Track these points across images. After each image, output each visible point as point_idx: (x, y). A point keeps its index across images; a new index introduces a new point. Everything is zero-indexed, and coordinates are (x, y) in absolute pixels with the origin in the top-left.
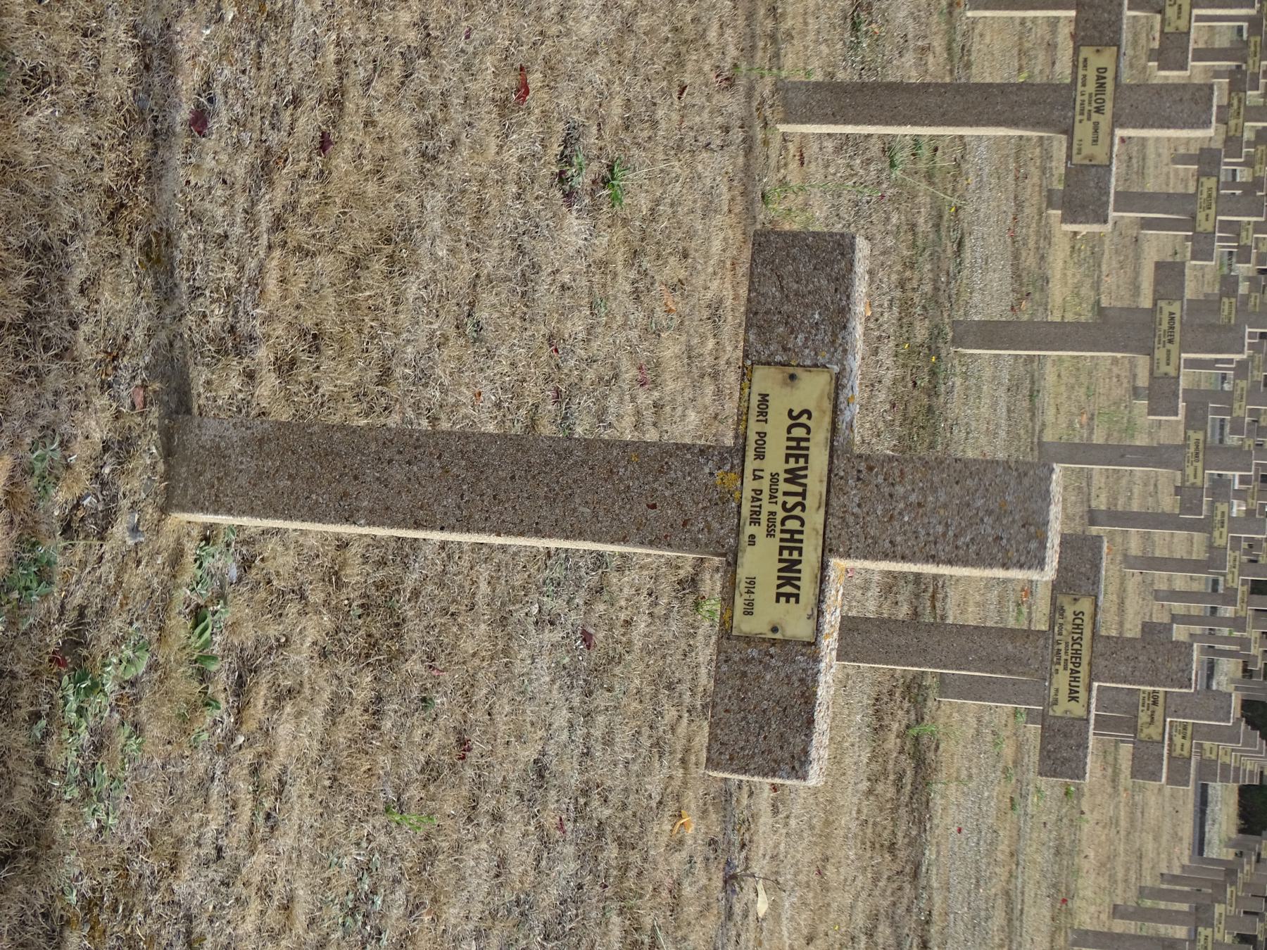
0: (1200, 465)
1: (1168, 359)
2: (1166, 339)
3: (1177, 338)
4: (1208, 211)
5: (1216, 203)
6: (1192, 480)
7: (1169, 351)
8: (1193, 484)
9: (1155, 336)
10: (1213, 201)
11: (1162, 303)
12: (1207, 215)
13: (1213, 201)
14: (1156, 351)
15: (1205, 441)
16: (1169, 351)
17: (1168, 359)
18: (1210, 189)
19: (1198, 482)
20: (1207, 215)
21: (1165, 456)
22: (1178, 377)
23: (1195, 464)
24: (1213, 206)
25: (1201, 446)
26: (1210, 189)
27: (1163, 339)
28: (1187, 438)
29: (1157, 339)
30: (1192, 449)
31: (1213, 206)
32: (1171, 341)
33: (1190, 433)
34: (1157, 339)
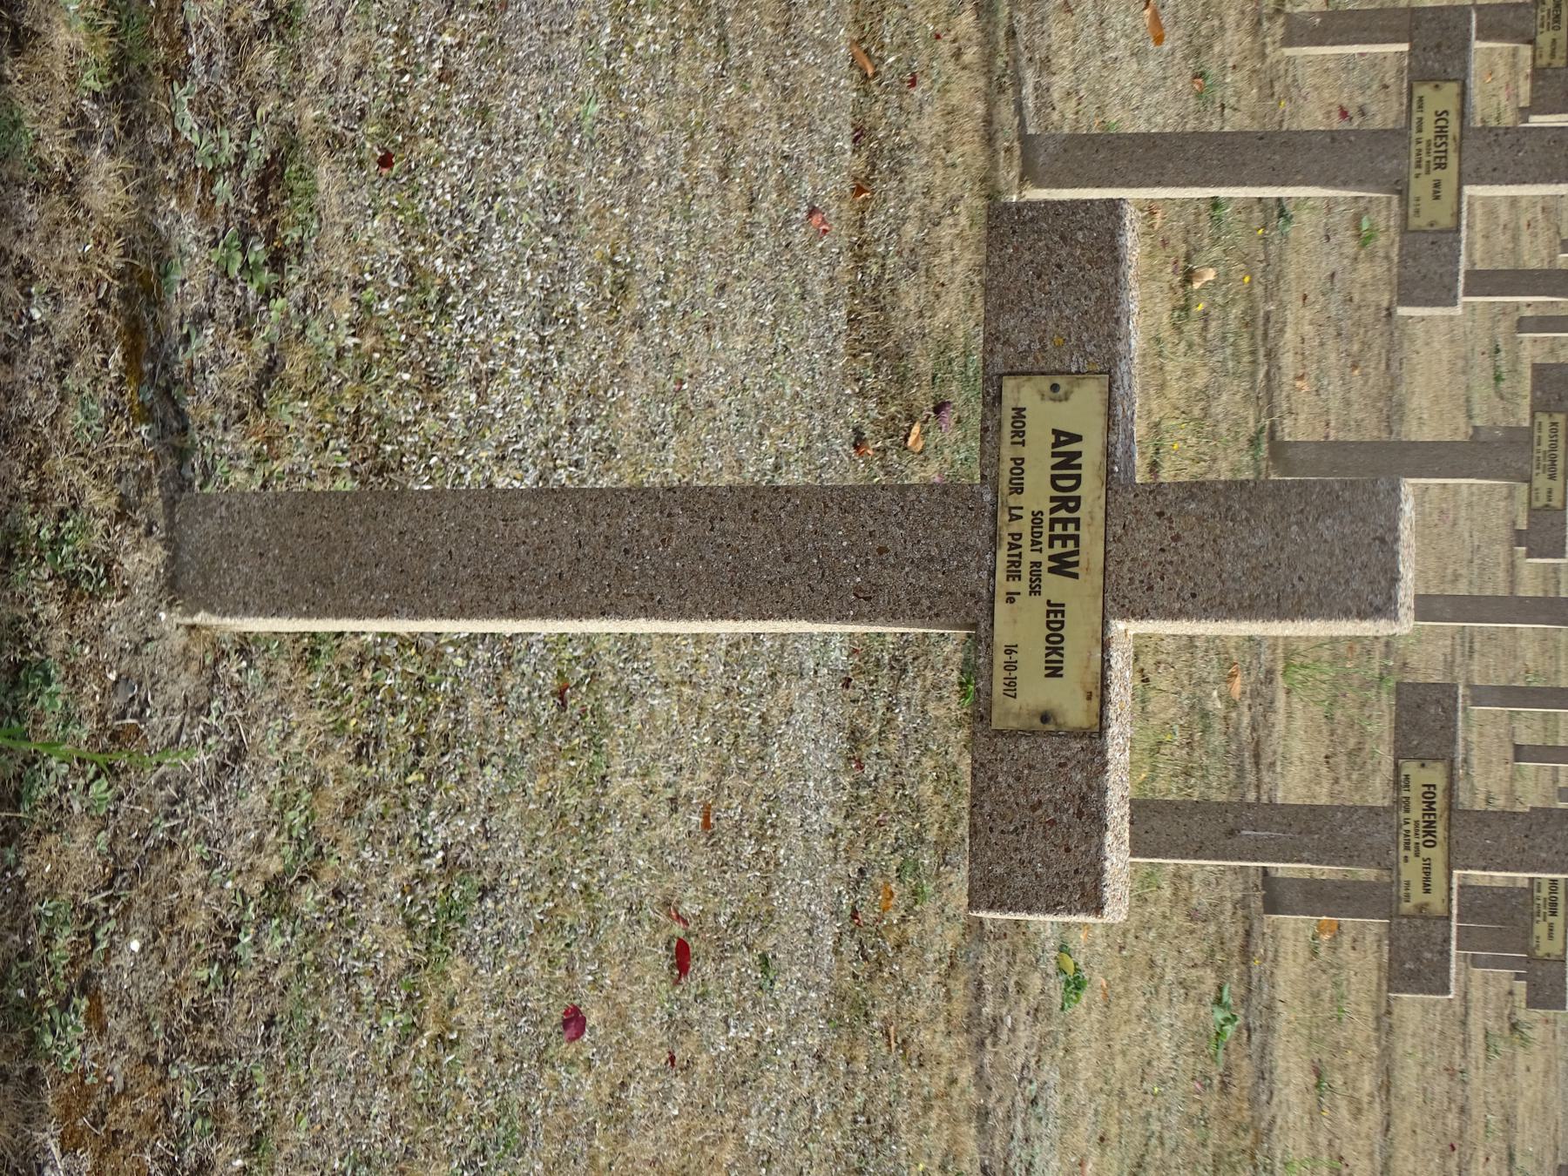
0: (1437, 855)
1: (1055, 646)
2: (1043, 558)
3: (1092, 549)
4: (1437, 174)
5: (1460, 150)
6: (1417, 895)
7: (1056, 611)
8: (1422, 907)
9: (994, 539)
10: (1452, 147)
11: (1023, 393)
12: (1437, 185)
13: (1452, 147)
14: (1001, 607)
15: (1450, 790)
16: (1056, 611)
17: (1055, 646)
18: (1441, 115)
19: (1436, 900)
20: (1437, 185)
21: (1347, 830)
22: (1102, 731)
23: (1425, 852)
24: (1453, 160)
25: (1440, 803)
26: (1441, 115)
27: (1028, 556)
28: (1399, 781)
29: (1003, 555)
30: (1416, 813)
31: (1453, 160)
32: (1063, 566)
33: (1410, 768)
34: (1003, 555)
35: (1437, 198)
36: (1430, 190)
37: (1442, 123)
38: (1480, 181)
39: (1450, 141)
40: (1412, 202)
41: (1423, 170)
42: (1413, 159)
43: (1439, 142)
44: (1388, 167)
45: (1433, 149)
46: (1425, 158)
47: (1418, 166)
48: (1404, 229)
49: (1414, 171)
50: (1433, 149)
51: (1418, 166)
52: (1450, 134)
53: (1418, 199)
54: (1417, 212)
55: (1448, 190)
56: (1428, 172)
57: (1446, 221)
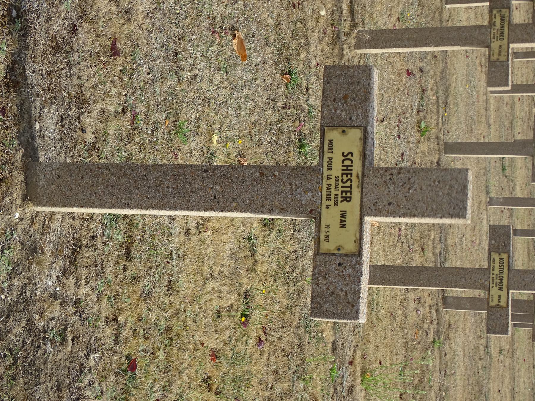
4: (343, 206)
5: (362, 187)
12: (343, 215)
20: (343, 215)
24: (356, 194)
31: (356, 194)
35: (343, 226)
36: (338, 219)
37: (347, 163)
38: (378, 213)
39: (354, 178)
40: (323, 229)
41: (332, 203)
42: (325, 193)
43: (345, 178)
44: (305, 198)
45: (341, 184)
46: (334, 192)
47: (329, 199)
48: (317, 253)
49: (325, 202)
50: (341, 184)
51: (329, 199)
52: (354, 173)
53: (328, 227)
54: (327, 237)
55: (352, 220)
56: (336, 204)
57: (350, 247)
